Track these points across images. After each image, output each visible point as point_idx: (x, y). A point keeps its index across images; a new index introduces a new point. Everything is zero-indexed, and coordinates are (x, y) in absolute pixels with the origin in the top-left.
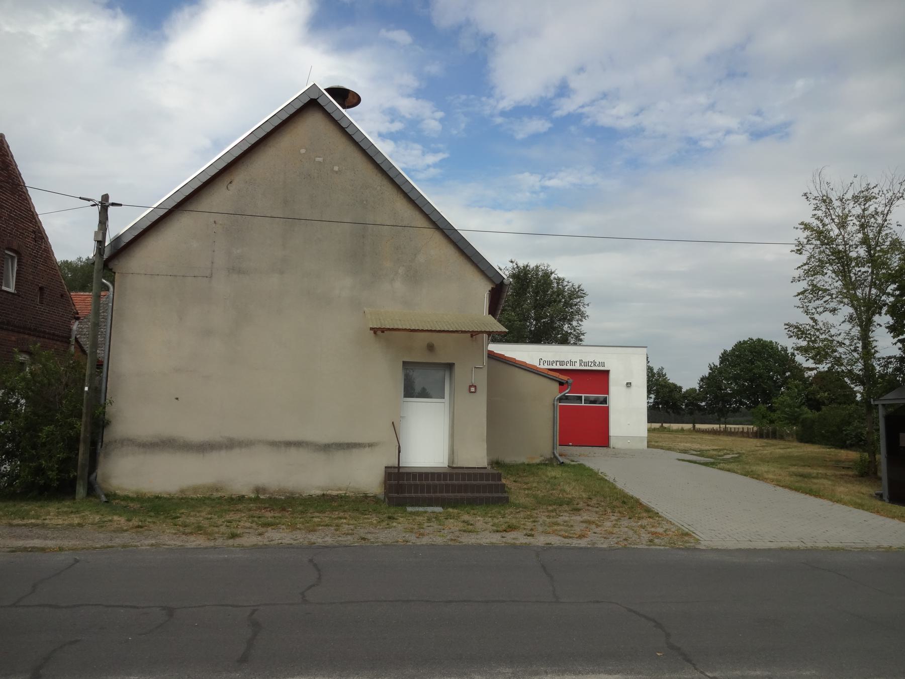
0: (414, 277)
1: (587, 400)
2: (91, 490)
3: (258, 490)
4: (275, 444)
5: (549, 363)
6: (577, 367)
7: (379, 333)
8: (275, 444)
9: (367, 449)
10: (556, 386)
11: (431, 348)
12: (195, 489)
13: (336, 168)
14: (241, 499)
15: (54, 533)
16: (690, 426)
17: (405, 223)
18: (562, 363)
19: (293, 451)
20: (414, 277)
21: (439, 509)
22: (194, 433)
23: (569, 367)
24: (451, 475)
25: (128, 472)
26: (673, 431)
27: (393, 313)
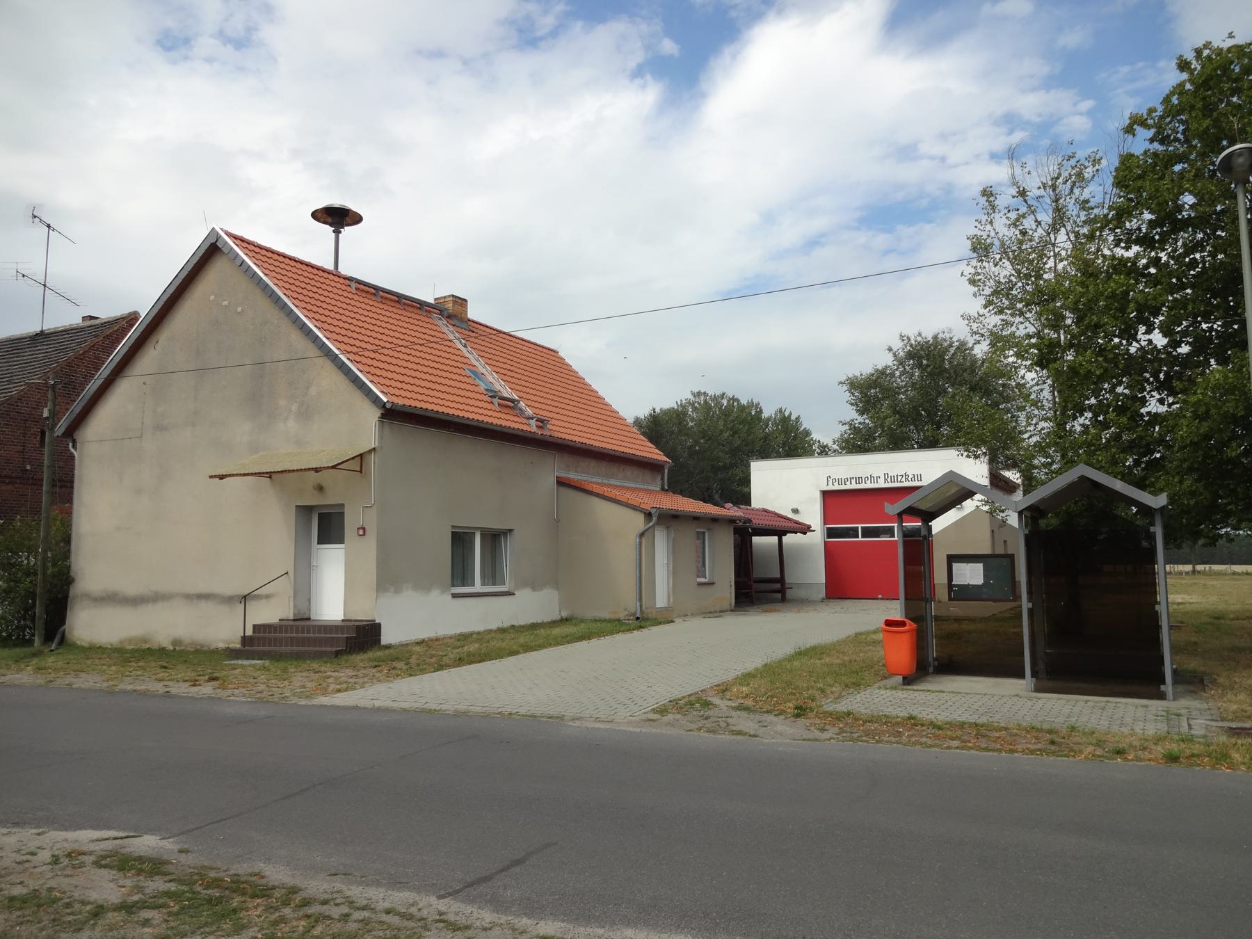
0: (306, 414)
1: (867, 532)
2: (63, 641)
3: (176, 642)
4: (188, 597)
5: (840, 481)
6: (881, 484)
7: (274, 476)
8: (188, 597)
9: (264, 601)
10: (640, 518)
11: (320, 488)
12: (130, 641)
13: (239, 309)
14: (163, 650)
15: (22, 676)
16: (1189, 568)
17: (299, 356)
18: (858, 480)
19: (204, 605)
20: (306, 414)
21: (267, 663)
22: (130, 587)
23: (869, 485)
24: (281, 627)
25: (89, 624)
26: (1239, 574)
27: (284, 455)
